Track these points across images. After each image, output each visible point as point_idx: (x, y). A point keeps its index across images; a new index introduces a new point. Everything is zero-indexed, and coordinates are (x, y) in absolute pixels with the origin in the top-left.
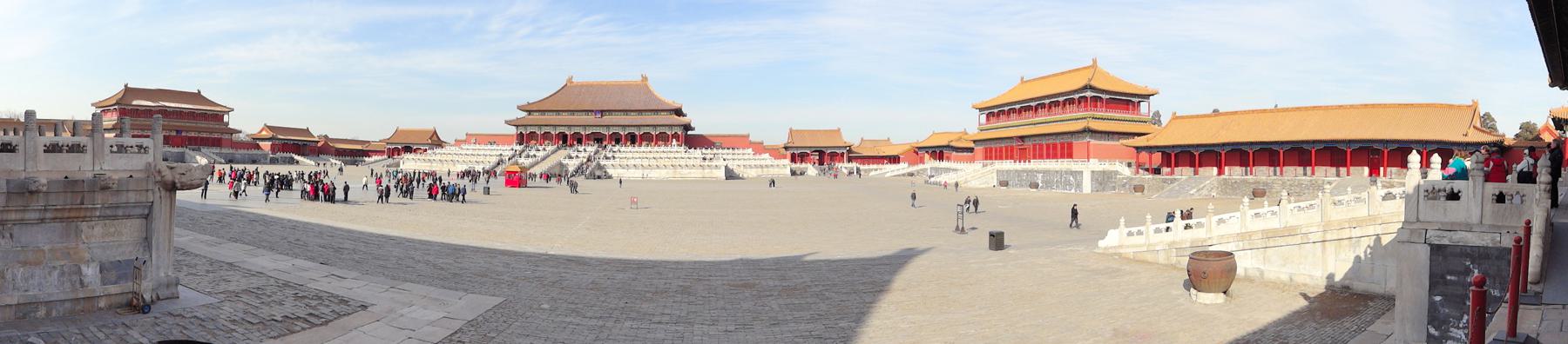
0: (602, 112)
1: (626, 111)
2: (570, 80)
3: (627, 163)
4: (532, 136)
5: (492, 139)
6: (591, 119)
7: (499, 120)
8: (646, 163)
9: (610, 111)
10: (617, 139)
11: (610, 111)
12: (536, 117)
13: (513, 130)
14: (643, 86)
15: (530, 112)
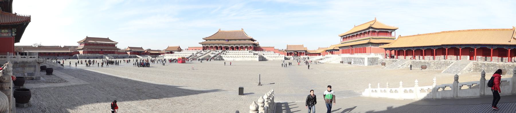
0: (228, 40)
1: (235, 40)
2: (220, 30)
3: (230, 56)
4: (207, 47)
5: (195, 49)
6: (225, 42)
7: (197, 42)
8: (234, 56)
9: (231, 40)
10: (233, 48)
11: (231, 40)
12: (208, 41)
13: (201, 46)
14: (242, 32)
15: (207, 40)
